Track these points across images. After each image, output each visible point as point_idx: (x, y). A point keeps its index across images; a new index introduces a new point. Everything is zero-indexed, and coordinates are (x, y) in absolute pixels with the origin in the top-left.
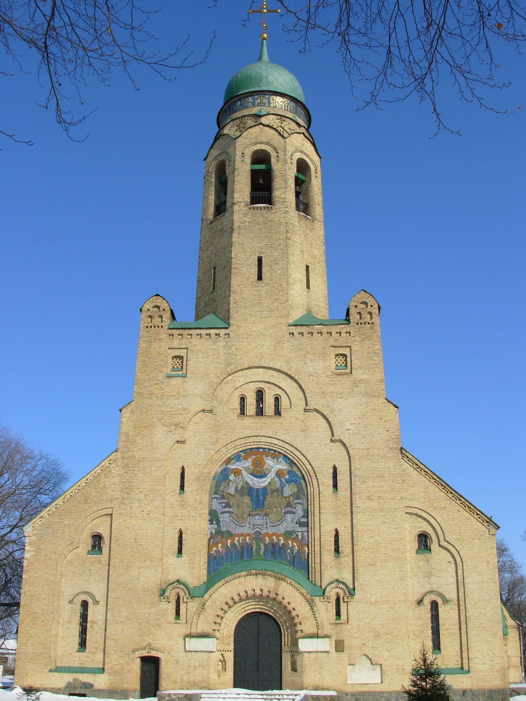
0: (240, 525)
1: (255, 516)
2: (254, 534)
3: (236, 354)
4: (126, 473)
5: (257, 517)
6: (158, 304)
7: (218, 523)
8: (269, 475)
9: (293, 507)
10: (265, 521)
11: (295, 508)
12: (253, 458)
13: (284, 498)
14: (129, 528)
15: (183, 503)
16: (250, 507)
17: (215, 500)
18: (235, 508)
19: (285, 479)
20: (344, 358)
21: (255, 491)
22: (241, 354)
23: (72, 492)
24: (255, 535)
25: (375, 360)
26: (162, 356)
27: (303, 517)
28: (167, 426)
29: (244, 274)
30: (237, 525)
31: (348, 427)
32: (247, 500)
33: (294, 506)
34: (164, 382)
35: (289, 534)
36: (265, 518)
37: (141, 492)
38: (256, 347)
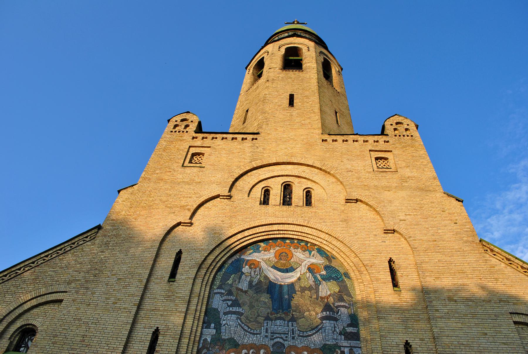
0: (252, 331)
1: (275, 321)
2: (273, 346)
3: (263, 153)
4: (102, 252)
5: (278, 322)
6: (188, 118)
7: (218, 327)
8: (298, 269)
9: (334, 312)
10: (291, 328)
11: (337, 313)
12: (276, 249)
13: (319, 298)
14: (80, 320)
15: (170, 294)
16: (269, 308)
17: (218, 296)
18: (246, 307)
19: (321, 275)
20: (386, 162)
21: (277, 288)
22: (269, 153)
23: (21, 268)
24: (275, 348)
25: (423, 162)
26: (181, 152)
27: (349, 326)
28: (170, 207)
29: (276, 103)
30: (247, 331)
31: (402, 218)
32: (265, 298)
33: (335, 309)
34: (178, 171)
35: (330, 349)
36: (290, 323)
37: (113, 275)
38: (286, 148)
